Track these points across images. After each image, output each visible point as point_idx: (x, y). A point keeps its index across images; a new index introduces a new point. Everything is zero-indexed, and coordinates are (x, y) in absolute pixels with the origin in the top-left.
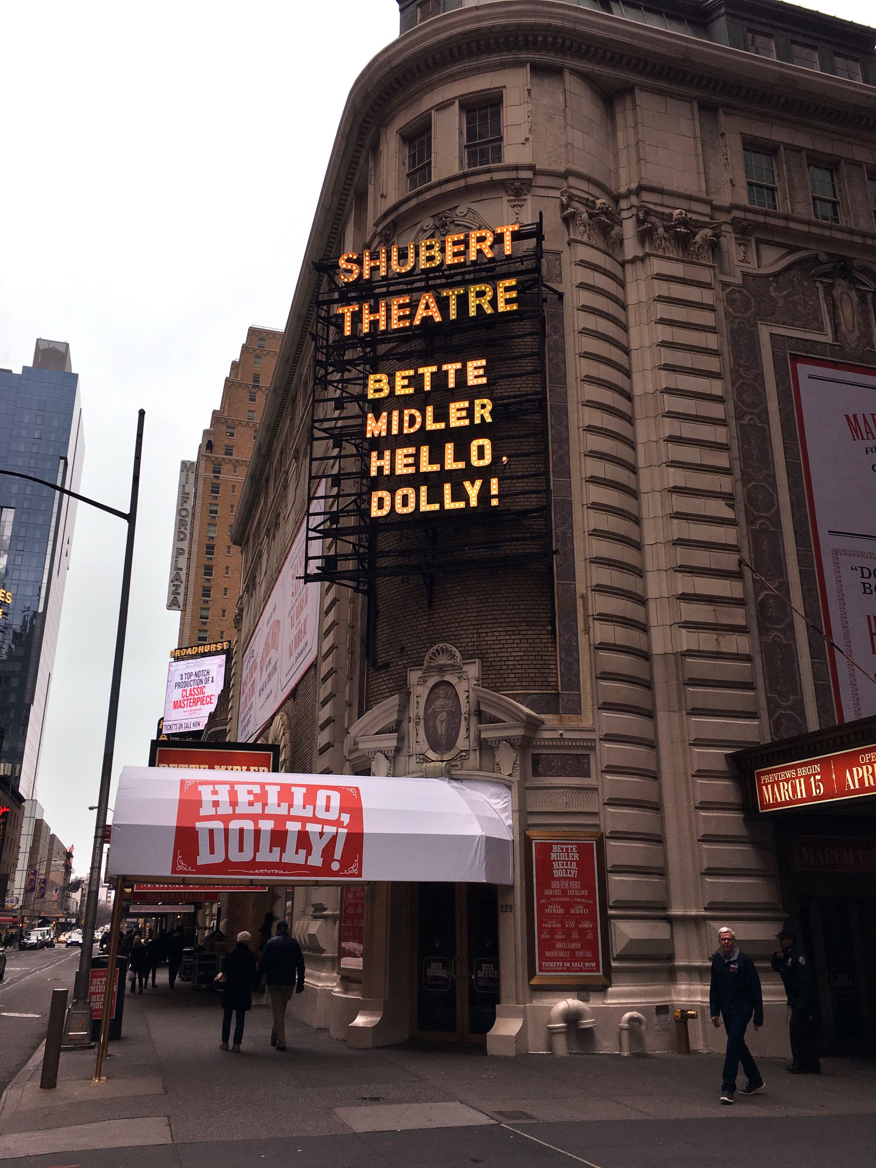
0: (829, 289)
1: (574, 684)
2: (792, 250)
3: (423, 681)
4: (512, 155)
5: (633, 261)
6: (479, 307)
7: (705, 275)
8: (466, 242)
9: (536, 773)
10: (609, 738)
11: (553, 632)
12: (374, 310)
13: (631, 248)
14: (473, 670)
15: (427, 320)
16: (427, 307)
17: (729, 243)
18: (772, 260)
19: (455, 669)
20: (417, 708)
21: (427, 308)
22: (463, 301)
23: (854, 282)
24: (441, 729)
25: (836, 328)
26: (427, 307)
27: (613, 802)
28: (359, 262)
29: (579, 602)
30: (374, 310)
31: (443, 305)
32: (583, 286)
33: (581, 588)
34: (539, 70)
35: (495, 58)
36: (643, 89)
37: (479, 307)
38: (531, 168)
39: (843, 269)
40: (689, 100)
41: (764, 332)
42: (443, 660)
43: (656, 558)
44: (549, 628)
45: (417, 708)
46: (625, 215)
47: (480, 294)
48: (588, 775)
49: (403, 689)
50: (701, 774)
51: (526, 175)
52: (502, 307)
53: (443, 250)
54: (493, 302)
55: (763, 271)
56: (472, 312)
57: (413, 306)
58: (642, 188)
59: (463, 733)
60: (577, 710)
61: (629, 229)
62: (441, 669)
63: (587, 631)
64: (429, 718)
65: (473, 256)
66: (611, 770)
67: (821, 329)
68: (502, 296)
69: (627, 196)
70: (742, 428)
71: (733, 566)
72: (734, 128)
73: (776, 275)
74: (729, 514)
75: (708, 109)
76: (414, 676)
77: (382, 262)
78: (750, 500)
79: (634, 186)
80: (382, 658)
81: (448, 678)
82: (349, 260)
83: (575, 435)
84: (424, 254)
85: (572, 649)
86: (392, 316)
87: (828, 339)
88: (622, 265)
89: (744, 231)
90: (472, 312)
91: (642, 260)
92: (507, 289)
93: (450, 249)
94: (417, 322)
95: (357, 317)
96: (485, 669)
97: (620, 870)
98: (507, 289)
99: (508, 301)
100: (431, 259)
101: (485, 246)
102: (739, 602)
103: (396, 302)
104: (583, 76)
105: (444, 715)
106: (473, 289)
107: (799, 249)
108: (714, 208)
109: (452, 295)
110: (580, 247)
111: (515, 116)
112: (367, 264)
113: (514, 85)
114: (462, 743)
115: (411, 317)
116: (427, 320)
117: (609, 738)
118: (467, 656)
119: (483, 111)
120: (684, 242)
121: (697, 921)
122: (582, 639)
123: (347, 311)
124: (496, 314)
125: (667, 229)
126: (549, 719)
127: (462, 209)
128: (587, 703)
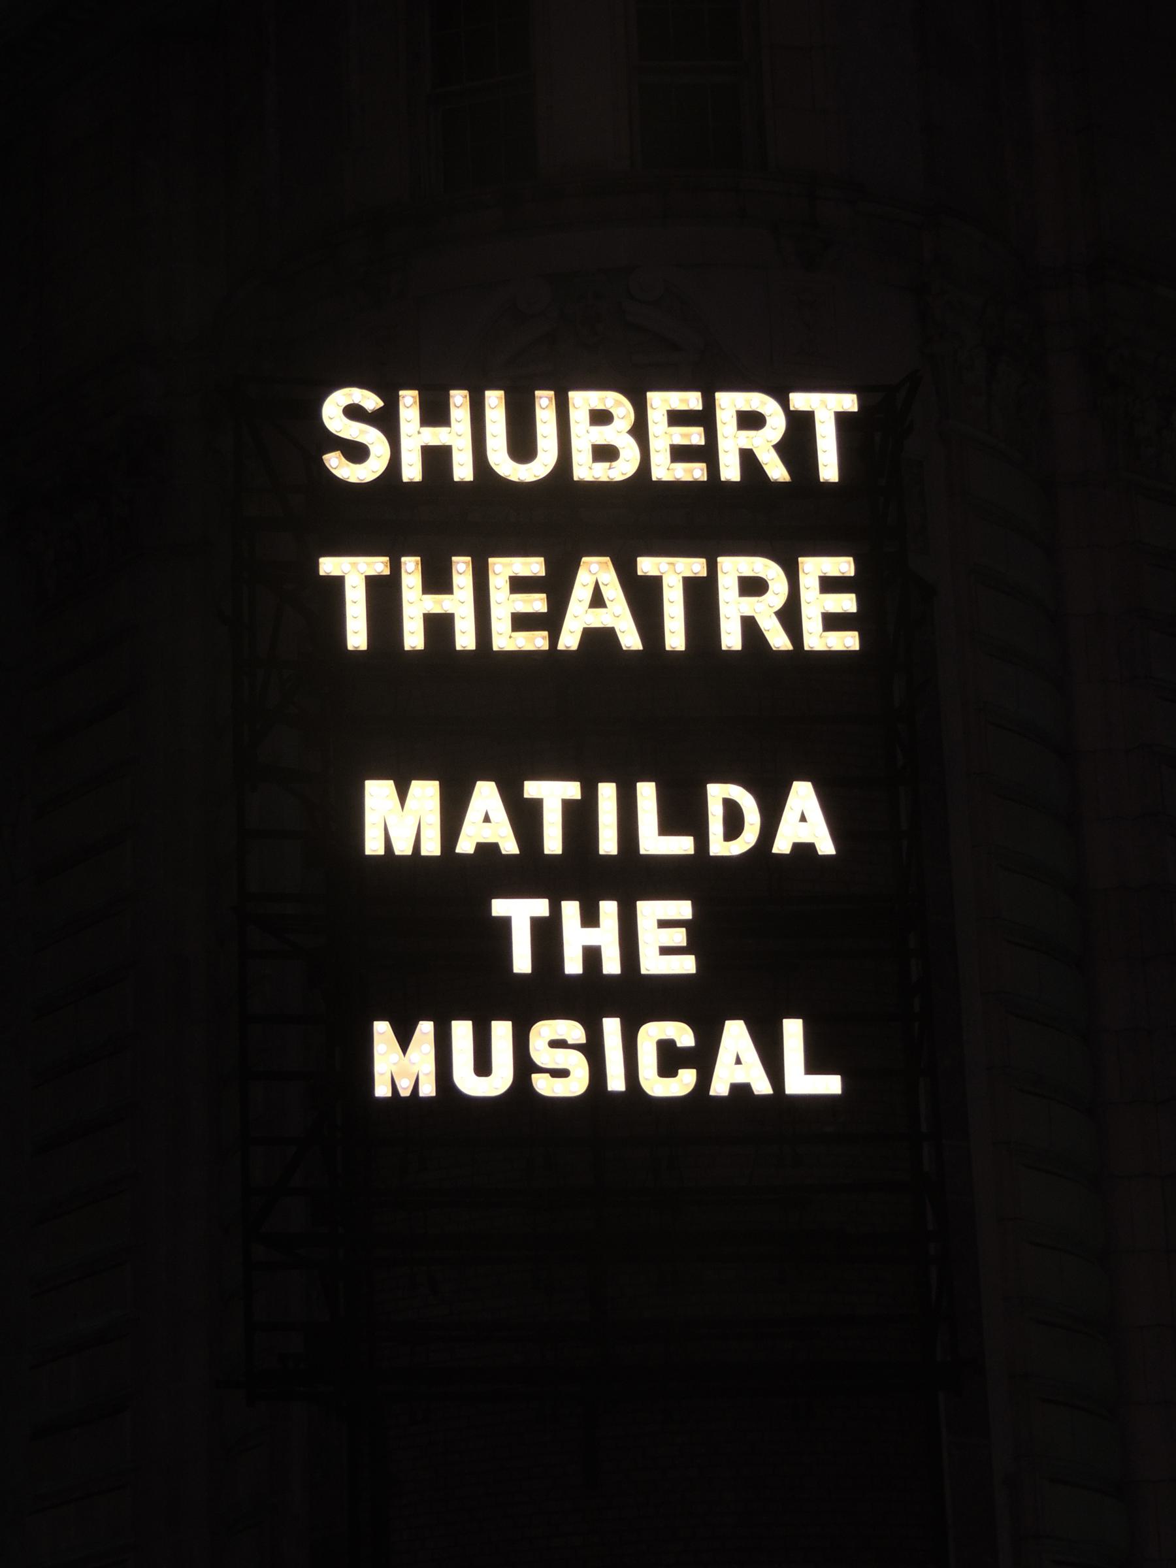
6: (750, 626)
8: (706, 418)
12: (437, 580)
16: (597, 600)
21: (598, 602)
22: (701, 595)
26: (597, 600)
28: (387, 421)
31: (644, 598)
37: (750, 626)
47: (753, 587)
52: (816, 639)
53: (640, 431)
54: (790, 616)
56: (731, 639)
65: (731, 471)
68: (816, 605)
77: (456, 435)
82: (354, 412)
84: (584, 436)
86: (488, 606)
90: (731, 639)
92: (830, 585)
93: (663, 436)
94: (569, 640)
98: (830, 585)
99: (833, 622)
100: (606, 453)
101: (765, 444)
103: (503, 569)
106: (733, 568)
109: (673, 572)
112: (415, 436)
115: (551, 622)
123: (354, 572)
124: (798, 654)
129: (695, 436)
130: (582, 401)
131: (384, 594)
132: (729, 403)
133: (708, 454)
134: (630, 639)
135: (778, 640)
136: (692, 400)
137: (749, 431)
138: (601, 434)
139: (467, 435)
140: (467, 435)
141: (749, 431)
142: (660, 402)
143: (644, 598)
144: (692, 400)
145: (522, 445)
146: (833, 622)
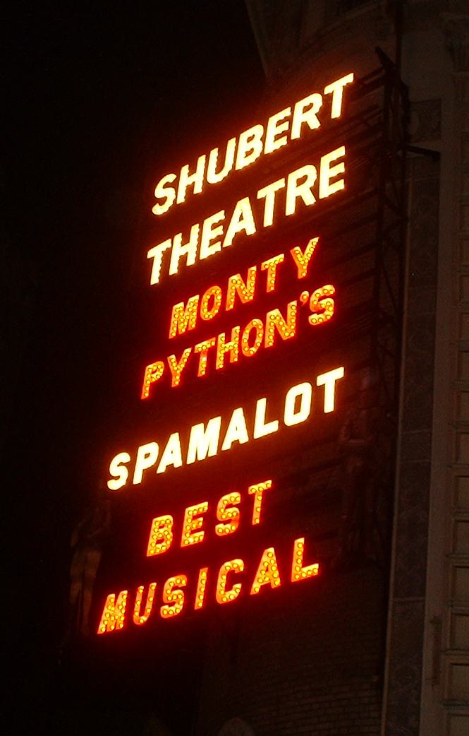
6: (299, 201)
11: (380, 685)
16: (241, 218)
21: (243, 220)
26: (241, 218)
44: (375, 679)
47: (301, 181)
52: (326, 191)
53: (263, 139)
86: (202, 242)
94: (228, 242)
99: (333, 181)
135: (310, 200)
137: (305, 114)
138: (249, 146)
139: (204, 173)
141: (305, 114)
146: (333, 181)
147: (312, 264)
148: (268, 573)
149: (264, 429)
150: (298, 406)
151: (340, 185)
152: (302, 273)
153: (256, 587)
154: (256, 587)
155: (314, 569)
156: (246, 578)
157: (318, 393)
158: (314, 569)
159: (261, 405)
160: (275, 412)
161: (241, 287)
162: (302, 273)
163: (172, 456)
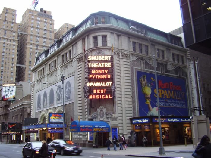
0: (141, 62)
1: (116, 111)
2: (137, 57)
3: (99, 110)
4: (109, 45)
5: (121, 59)
7: (128, 61)
9: (112, 120)
10: (119, 117)
11: (114, 105)
13: (121, 57)
14: (105, 109)
15: (100, 67)
17: (131, 56)
18: (135, 58)
19: (103, 109)
20: (99, 113)
21: (100, 65)
22: (104, 65)
23: (143, 61)
24: (102, 116)
25: (141, 67)
27: (119, 123)
29: (116, 102)
30: (93, 64)
31: (102, 65)
32: (117, 63)
33: (116, 100)
34: (111, 33)
35: (106, 31)
36: (123, 35)
38: (111, 47)
39: (142, 59)
40: (127, 37)
41: (134, 68)
42: (102, 108)
43: (123, 96)
45: (99, 113)
46: (120, 52)
48: (117, 120)
49: (96, 110)
50: (127, 120)
51: (110, 48)
52: (109, 67)
54: (108, 66)
55: (134, 60)
57: (98, 64)
58: (122, 50)
59: (104, 116)
60: (116, 114)
61: (120, 54)
62: (101, 109)
63: (117, 105)
64: (100, 114)
66: (120, 120)
67: (139, 67)
69: (120, 50)
70: (132, 80)
71: (131, 97)
72: (132, 40)
73: (135, 60)
74: (130, 91)
75: (129, 38)
76: (98, 109)
77: (94, 58)
78: (132, 89)
79: (121, 49)
80: (93, 107)
81: (102, 110)
83: (116, 82)
84: (99, 58)
85: (115, 107)
86: (95, 65)
87: (140, 68)
88: (120, 59)
89: (132, 54)
91: (122, 59)
94: (99, 67)
95: (91, 65)
96: (107, 109)
97: (120, 130)
102: (131, 101)
104: (116, 34)
105: (102, 114)
106: (105, 64)
107: (138, 57)
108: (130, 52)
110: (116, 58)
111: (109, 39)
113: (108, 34)
114: (104, 117)
115: (98, 66)
116: (100, 67)
117: (119, 117)
118: (105, 108)
119: (104, 37)
120: (126, 57)
121: (126, 134)
122: (116, 106)
124: (108, 67)
125: (125, 55)
126: (113, 115)
127: (102, 51)
128: (117, 113)
129: (104, 58)
130: (99, 56)
131: (91, 65)
132: (105, 57)
133: (104, 59)
134: (101, 67)
136: (104, 56)
140: (95, 58)
142: (103, 56)
143: (102, 65)
144: (104, 56)
145: (97, 59)
147: (107, 72)
148: (107, 97)
149: (104, 85)
150: (108, 84)
151: (110, 67)
152: (106, 73)
153: (106, 98)
154: (106, 98)
155: (111, 98)
156: (105, 97)
157: (109, 84)
158: (111, 98)
159: (104, 83)
160: (105, 84)
161: (100, 72)
162: (106, 73)
163: (95, 84)
